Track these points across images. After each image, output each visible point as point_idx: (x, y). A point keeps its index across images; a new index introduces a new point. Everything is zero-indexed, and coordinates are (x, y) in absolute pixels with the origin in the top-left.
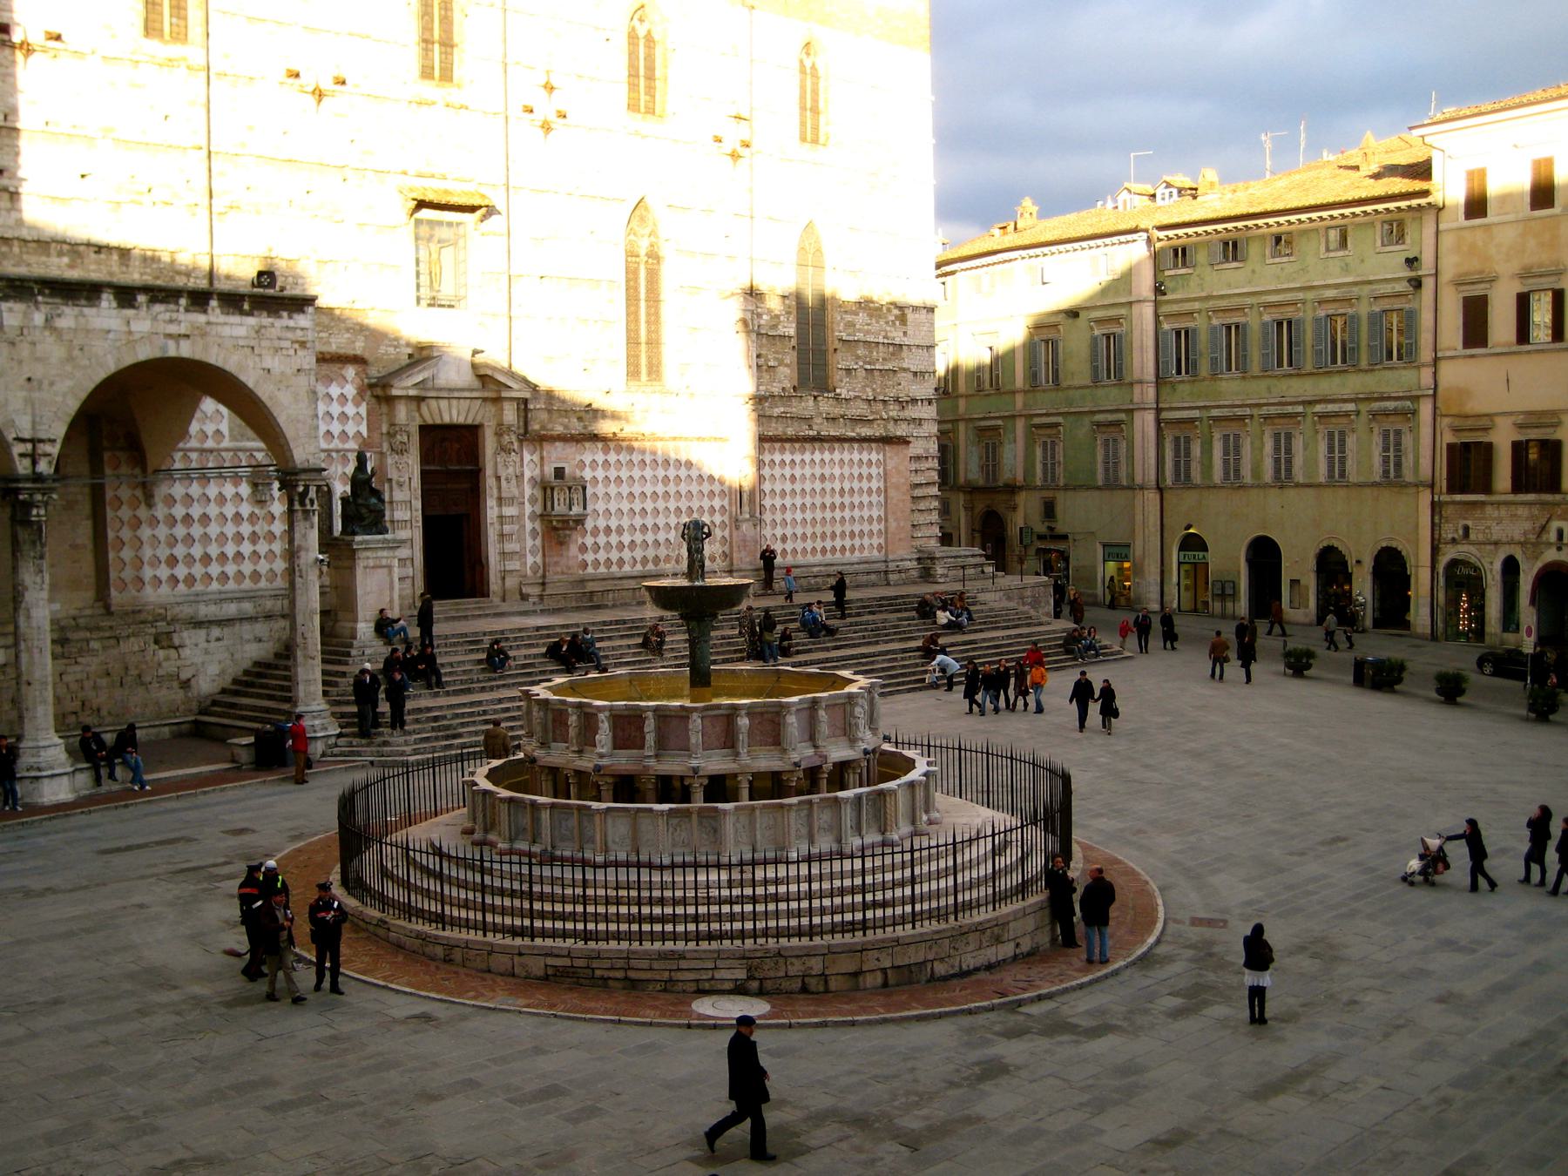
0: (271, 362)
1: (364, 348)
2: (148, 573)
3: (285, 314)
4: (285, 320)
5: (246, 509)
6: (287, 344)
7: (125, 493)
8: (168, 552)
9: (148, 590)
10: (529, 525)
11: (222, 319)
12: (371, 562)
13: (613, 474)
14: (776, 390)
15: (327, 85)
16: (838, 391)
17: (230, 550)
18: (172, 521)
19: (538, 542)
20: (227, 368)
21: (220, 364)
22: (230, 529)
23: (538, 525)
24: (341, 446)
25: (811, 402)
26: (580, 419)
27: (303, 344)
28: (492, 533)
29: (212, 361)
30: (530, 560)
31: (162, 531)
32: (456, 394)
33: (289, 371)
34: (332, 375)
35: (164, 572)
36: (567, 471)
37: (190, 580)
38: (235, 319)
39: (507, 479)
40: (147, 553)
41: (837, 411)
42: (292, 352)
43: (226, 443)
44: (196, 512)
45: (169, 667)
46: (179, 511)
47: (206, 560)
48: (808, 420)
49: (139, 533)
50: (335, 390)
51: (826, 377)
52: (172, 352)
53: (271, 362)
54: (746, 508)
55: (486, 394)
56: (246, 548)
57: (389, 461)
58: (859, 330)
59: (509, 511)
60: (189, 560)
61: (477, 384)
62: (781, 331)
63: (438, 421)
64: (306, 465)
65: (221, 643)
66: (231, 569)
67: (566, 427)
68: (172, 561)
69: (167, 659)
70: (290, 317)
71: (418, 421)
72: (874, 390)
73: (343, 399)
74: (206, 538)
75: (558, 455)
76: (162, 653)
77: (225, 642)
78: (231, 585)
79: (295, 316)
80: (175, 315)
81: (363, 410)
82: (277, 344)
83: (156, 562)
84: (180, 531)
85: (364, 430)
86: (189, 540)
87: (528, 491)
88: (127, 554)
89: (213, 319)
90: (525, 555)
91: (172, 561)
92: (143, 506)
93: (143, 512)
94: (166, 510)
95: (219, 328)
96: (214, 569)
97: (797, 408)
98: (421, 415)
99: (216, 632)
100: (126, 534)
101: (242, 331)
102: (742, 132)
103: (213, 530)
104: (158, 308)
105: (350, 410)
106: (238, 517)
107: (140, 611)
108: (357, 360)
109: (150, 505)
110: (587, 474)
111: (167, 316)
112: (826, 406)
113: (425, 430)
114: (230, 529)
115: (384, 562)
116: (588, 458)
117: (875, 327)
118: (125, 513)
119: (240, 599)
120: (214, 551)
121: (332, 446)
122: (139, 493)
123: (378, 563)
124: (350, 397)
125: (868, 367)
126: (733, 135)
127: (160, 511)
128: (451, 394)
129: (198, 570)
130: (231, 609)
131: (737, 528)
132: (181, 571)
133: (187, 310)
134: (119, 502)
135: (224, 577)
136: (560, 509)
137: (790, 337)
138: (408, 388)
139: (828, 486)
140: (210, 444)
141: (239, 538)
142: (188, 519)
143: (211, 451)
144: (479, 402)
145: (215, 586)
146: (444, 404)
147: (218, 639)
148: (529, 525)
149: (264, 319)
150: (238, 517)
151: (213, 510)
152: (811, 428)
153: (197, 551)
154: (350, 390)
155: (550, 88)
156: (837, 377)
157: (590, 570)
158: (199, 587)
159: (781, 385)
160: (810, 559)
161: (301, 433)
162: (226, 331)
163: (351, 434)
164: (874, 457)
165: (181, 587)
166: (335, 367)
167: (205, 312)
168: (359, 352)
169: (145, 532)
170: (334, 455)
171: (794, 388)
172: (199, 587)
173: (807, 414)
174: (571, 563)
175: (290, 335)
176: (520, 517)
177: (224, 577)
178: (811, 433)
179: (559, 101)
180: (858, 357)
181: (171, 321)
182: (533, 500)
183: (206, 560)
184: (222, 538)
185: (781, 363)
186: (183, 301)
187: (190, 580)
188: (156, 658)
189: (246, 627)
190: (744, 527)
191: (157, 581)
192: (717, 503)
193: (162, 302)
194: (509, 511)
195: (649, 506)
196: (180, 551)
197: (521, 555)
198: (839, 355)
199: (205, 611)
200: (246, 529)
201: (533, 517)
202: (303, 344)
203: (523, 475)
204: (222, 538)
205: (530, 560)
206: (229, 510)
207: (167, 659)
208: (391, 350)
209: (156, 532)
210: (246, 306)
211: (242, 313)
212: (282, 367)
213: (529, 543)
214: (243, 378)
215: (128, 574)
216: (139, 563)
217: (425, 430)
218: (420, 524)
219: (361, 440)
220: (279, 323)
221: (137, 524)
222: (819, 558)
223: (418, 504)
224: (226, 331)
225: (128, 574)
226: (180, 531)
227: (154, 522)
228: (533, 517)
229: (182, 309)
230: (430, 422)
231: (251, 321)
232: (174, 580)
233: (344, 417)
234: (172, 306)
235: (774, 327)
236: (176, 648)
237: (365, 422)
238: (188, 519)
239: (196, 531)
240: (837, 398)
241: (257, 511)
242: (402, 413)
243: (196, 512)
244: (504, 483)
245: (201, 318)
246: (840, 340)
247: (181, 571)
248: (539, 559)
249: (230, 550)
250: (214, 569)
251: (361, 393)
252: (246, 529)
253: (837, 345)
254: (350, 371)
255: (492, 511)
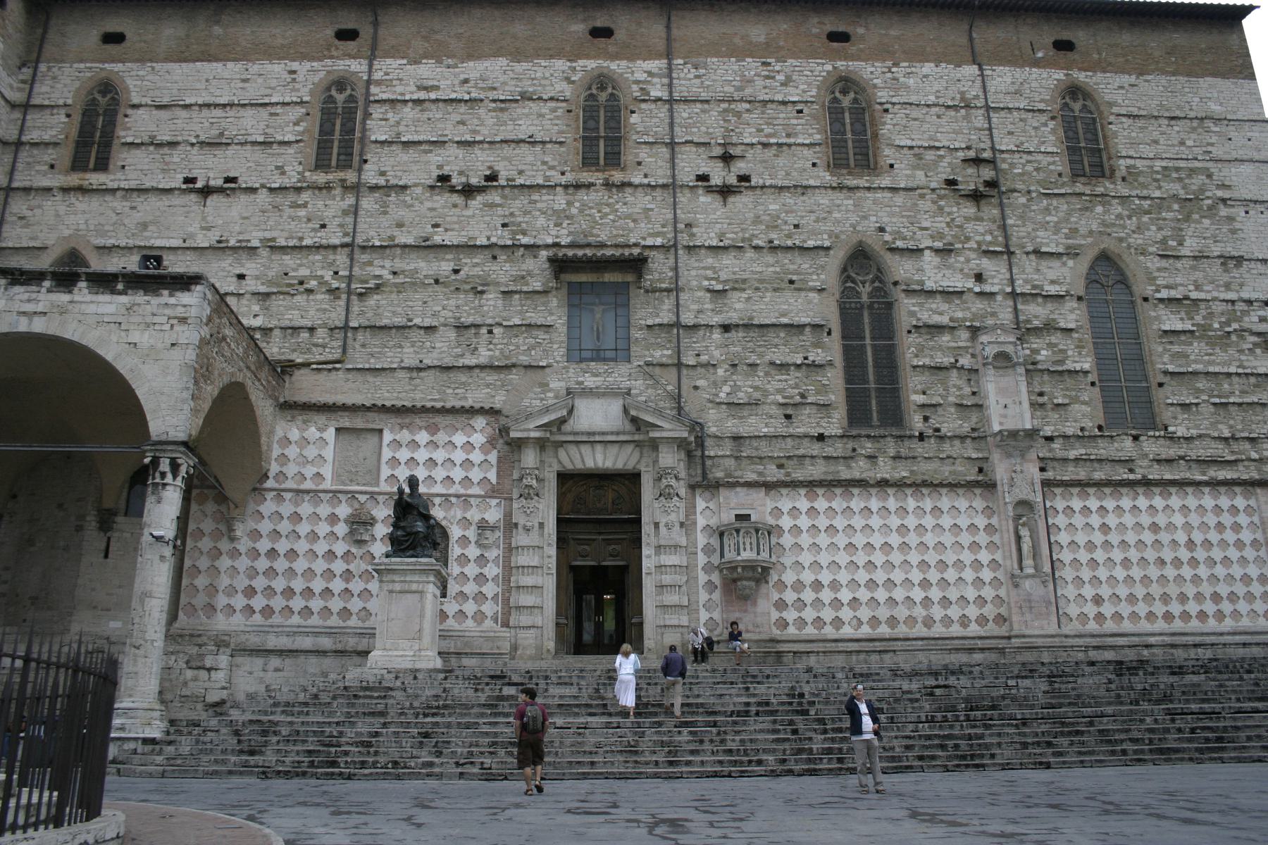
0: (144, 338)
1: (504, 402)
2: (222, 600)
3: (166, 292)
4: (165, 297)
5: (340, 548)
6: (164, 319)
7: (208, 525)
8: (247, 582)
9: (220, 617)
10: (702, 578)
11: (89, 297)
12: (398, 587)
13: (822, 522)
14: (1070, 432)
15: (474, 181)
16: (1171, 429)
17: (318, 585)
18: (254, 554)
19: (717, 596)
20: (84, 342)
21: (76, 338)
22: (320, 566)
23: (716, 578)
24: (462, 491)
25: (1128, 442)
26: (780, 466)
27: (183, 320)
28: (648, 584)
29: (68, 335)
30: (704, 616)
31: (243, 563)
32: (597, 438)
33: (160, 345)
34: (458, 425)
35: (239, 601)
36: (753, 518)
37: (268, 611)
38: (107, 298)
39: (667, 525)
40: (224, 581)
41: (1172, 452)
42: (167, 327)
43: (327, 485)
44: (282, 546)
45: (194, 688)
46: (264, 545)
47: (289, 593)
48: (1128, 463)
49: (217, 564)
50: (459, 439)
51: (1153, 416)
52: (23, 326)
53: (144, 338)
54: (1028, 562)
55: (636, 437)
56: (337, 585)
57: (515, 505)
58: (1196, 362)
59: (670, 559)
60: (270, 592)
61: (628, 426)
62: (1070, 365)
63: (579, 466)
64: (164, 438)
65: (280, 674)
66: (316, 604)
67: (760, 474)
68: (250, 592)
69: (195, 679)
70: (171, 295)
71: (556, 467)
72: (1231, 427)
73: (469, 446)
74: (291, 572)
75: (733, 502)
76: (189, 674)
77: (285, 674)
78: (315, 620)
79: (179, 294)
80: (34, 296)
81: (493, 457)
82: (149, 319)
83: (231, 591)
84: (262, 564)
85: (492, 476)
86: (271, 572)
87: (702, 540)
88: (201, 581)
89: (77, 298)
90: (697, 611)
91: (250, 592)
92: (226, 538)
93: (224, 545)
94: (251, 544)
95: (83, 306)
96: (297, 603)
97: (1103, 449)
98: (560, 462)
99: (275, 662)
100: (203, 563)
101: (111, 309)
102: (987, 173)
103: (300, 565)
104: (18, 289)
105: (477, 457)
106: (331, 555)
107: (200, 636)
108: (493, 412)
109: (232, 539)
110: (786, 522)
111: (26, 296)
112: (1151, 447)
113: (564, 478)
114: (320, 566)
115: (414, 587)
116: (786, 505)
117: (1221, 356)
118: (206, 544)
119: (317, 634)
120: (298, 585)
121: (452, 491)
122: (223, 528)
123: (406, 587)
124: (477, 445)
125: (1217, 400)
126: (971, 179)
127: (244, 545)
128: (591, 440)
129: (278, 603)
130: (307, 643)
131: (1016, 586)
132: (258, 602)
133: (49, 291)
134: (200, 533)
135: (306, 611)
136: (730, 555)
137: (1086, 373)
138: (529, 430)
139: (1165, 537)
140: (308, 485)
141: (329, 575)
142: (272, 553)
143: (308, 492)
144: (630, 448)
145: (295, 619)
146: (586, 450)
147: (277, 670)
148: (702, 578)
149: (140, 298)
150: (331, 555)
151: (302, 546)
152: (1131, 471)
153: (279, 584)
154: (478, 439)
155: (727, 158)
156: (1166, 415)
157: (792, 630)
158: (276, 619)
159: (1078, 425)
160: (1145, 626)
161: (163, 406)
162: (92, 309)
163: (476, 481)
164: (1240, 502)
165: (257, 618)
166: (462, 419)
167: (70, 292)
168: (497, 406)
169: (225, 563)
170: (453, 500)
171: (1100, 428)
172: (276, 619)
173: (1123, 455)
174: (759, 620)
175: (168, 312)
176: (688, 569)
177: (306, 611)
178: (1132, 477)
179: (740, 167)
180: (1199, 391)
181: (29, 301)
182: (708, 550)
183: (289, 593)
184: (309, 573)
185: (1076, 400)
186: (47, 284)
187: (268, 611)
188: (182, 678)
189: (313, 660)
190: (1027, 584)
191: (230, 609)
192: (984, 557)
193: (22, 284)
194: (670, 559)
195: (879, 558)
196: (260, 583)
197: (690, 608)
198: (1167, 389)
199: (273, 642)
200: (339, 566)
201: (708, 568)
202: (183, 320)
203: (695, 523)
204: (309, 573)
205: (704, 616)
206: (321, 548)
207: (195, 679)
208: (538, 403)
209: (236, 564)
210: (120, 286)
211: (114, 292)
212: (152, 341)
213: (703, 596)
214: (101, 352)
215: (200, 600)
216: (212, 589)
217: (564, 478)
218: (554, 571)
219: (489, 487)
220: (155, 301)
221: (216, 554)
222: (1161, 625)
223: (552, 551)
224: (92, 309)
225: (200, 600)
226: (262, 564)
227: (235, 554)
228: (708, 568)
229: (44, 290)
230: (569, 466)
231: (123, 299)
232: (249, 610)
233: (467, 464)
234: (34, 288)
235: (1062, 362)
236: (209, 670)
237: (494, 470)
238: (272, 553)
239: (281, 565)
240: (1172, 438)
241: (354, 550)
242: (530, 458)
243: (282, 546)
244: (663, 529)
245: (64, 298)
246: (1166, 373)
247: (258, 602)
248: (716, 615)
249: (318, 585)
250: (297, 603)
251: (491, 442)
252: (339, 566)
253: (1161, 378)
254: (480, 422)
255: (649, 560)
